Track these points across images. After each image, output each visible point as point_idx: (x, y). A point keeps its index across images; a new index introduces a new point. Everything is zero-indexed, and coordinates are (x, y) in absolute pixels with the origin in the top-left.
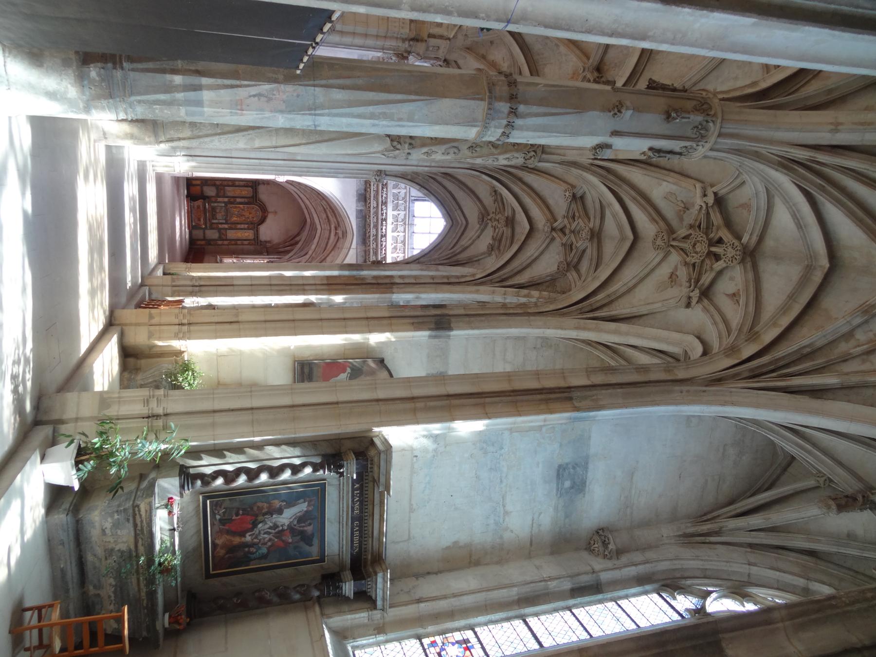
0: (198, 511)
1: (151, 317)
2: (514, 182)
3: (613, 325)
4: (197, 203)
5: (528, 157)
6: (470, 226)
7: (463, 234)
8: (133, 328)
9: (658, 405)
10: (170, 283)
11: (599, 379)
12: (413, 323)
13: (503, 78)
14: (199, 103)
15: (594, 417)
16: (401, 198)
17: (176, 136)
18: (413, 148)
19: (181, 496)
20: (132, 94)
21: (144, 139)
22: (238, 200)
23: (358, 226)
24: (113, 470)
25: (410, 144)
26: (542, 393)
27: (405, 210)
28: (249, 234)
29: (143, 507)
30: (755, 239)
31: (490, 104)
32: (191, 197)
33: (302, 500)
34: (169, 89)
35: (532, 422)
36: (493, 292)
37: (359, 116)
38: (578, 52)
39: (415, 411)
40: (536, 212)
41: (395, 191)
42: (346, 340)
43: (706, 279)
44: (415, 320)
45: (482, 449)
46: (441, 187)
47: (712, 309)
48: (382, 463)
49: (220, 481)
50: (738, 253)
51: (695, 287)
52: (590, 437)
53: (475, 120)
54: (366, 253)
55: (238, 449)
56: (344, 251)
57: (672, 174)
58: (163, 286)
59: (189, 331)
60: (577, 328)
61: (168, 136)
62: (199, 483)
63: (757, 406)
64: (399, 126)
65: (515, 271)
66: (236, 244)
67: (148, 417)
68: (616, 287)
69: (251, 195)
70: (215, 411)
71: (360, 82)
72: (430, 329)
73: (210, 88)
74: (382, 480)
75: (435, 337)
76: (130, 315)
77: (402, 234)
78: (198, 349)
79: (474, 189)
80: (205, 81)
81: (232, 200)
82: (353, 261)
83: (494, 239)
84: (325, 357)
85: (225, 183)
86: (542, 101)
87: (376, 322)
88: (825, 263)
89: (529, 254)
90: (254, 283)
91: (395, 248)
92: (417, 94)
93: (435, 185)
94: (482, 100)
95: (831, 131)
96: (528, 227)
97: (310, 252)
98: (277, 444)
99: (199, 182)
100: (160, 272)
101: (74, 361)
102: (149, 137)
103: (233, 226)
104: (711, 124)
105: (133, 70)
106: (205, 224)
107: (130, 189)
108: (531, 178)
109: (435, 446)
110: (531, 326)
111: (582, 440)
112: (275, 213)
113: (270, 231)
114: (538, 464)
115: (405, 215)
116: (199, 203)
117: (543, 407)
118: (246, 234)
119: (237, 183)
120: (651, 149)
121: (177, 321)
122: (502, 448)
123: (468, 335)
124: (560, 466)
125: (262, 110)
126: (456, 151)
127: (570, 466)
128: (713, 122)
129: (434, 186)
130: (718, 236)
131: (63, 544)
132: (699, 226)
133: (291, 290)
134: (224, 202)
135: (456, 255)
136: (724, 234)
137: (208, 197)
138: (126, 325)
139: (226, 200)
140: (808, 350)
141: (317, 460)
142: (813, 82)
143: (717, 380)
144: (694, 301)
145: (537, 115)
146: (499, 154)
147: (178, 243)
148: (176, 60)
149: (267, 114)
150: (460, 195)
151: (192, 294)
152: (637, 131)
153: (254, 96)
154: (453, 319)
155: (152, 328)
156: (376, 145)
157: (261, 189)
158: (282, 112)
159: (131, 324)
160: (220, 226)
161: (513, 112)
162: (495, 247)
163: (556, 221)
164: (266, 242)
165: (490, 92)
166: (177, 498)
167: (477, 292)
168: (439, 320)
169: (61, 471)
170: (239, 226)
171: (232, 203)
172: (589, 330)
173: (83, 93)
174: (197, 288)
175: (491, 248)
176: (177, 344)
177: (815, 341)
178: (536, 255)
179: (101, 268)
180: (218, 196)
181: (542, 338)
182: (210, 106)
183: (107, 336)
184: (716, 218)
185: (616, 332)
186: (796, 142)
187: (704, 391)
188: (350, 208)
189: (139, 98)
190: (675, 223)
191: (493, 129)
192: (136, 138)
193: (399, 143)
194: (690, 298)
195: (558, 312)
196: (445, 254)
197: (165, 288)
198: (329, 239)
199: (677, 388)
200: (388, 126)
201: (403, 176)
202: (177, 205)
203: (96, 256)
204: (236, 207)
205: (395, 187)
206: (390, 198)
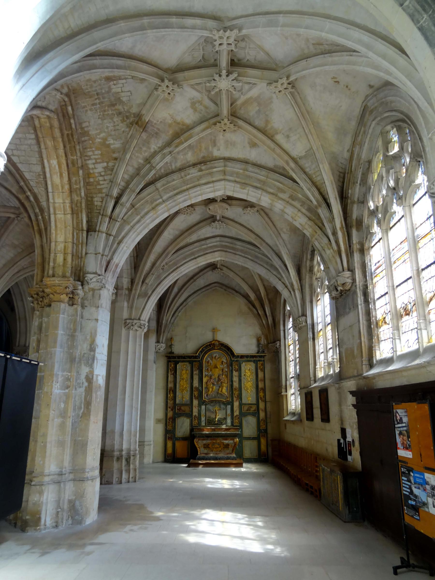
4: (201, 451)
22: (196, 383)
28: (248, 369)
66: (264, 390)
81: (196, 393)
85: (170, 403)
99: (170, 444)
103: (236, 393)
106: (233, 436)
112: (214, 330)
113: (243, 338)
116: (199, 444)
118: (248, 374)
119: (171, 385)
134: (200, 406)
137: (192, 430)
139: (195, 402)
160: (236, 413)
164: (259, 344)
170: (236, 385)
180: (190, 415)
198: (246, 162)
204: (207, 388)
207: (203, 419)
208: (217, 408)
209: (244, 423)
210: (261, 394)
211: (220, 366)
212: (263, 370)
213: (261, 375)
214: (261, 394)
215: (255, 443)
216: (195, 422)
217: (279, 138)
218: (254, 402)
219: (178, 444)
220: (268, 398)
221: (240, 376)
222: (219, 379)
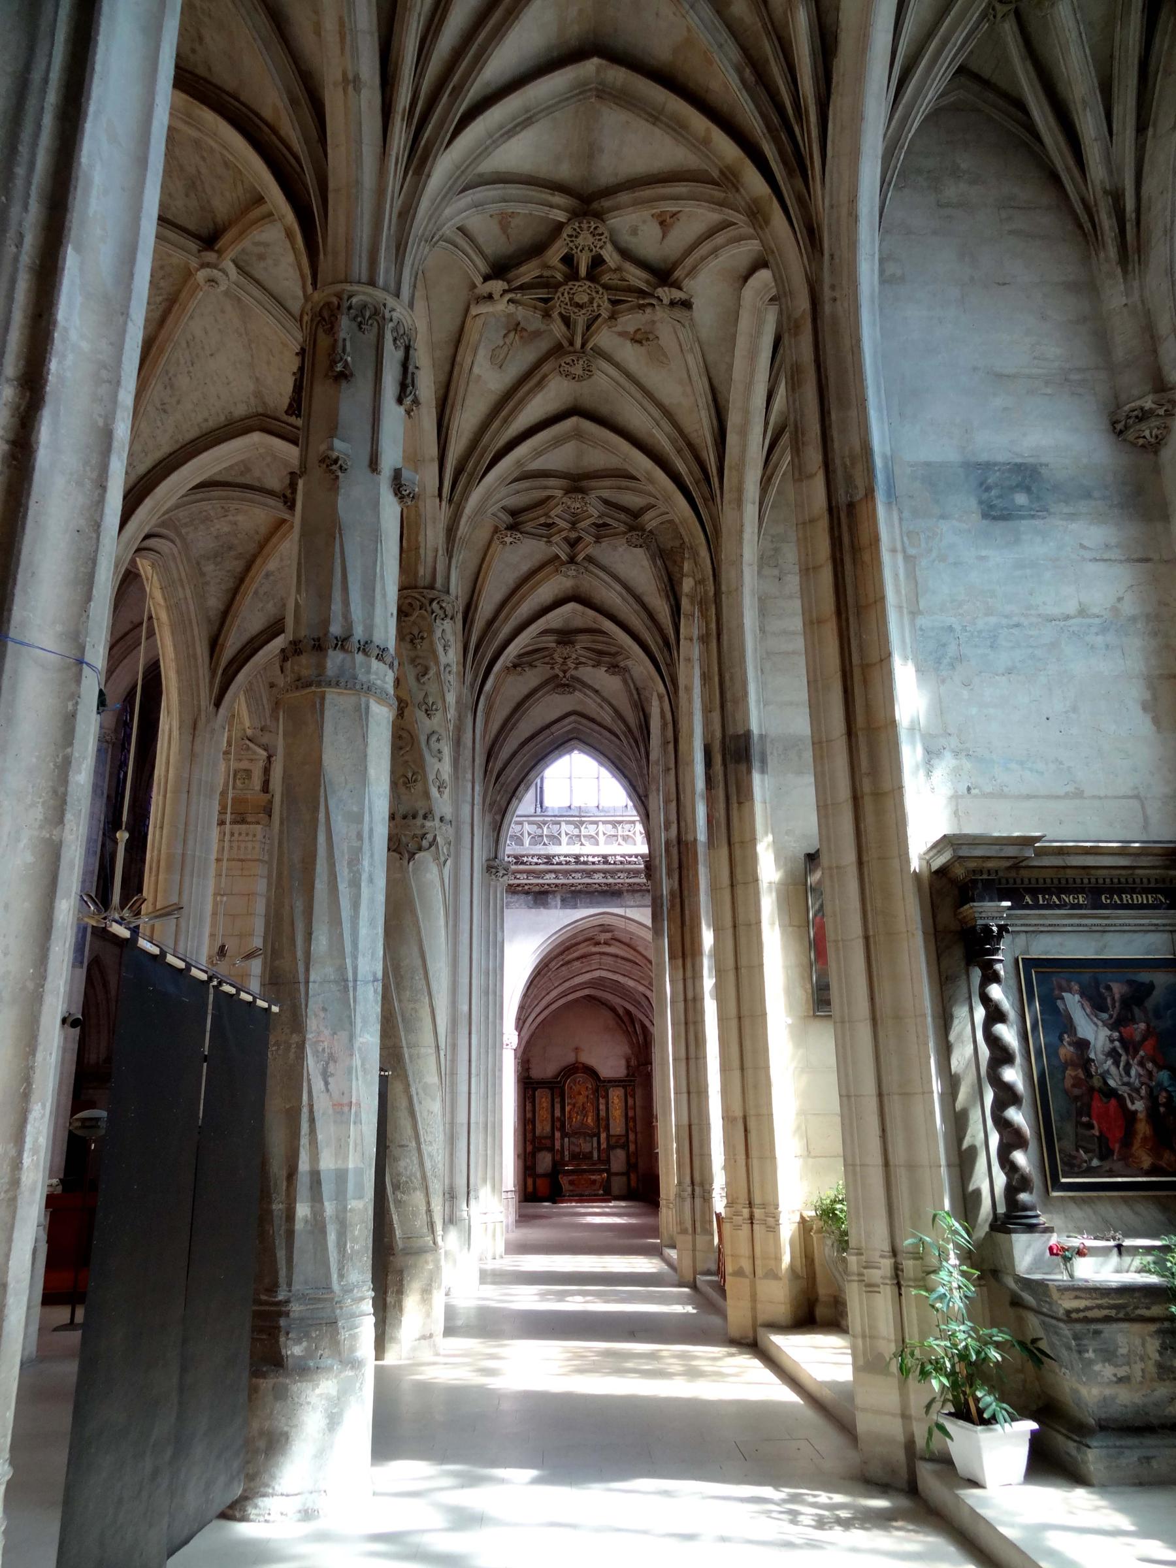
0: (1084, 1200)
1: (739, 1273)
2: (496, 634)
3: (732, 439)
5: (441, 613)
6: (578, 708)
7: (593, 720)
8: (759, 1306)
9: (859, 340)
10: (689, 1238)
11: (813, 457)
12: (740, 803)
13: (288, 664)
14: (341, 1176)
15: (884, 457)
16: (539, 832)
17: (423, 1216)
18: (431, 811)
19: (1049, 1230)
20: (328, 1288)
21: (431, 1271)
22: (558, 1113)
23: (591, 905)
24: (995, 1355)
25: (425, 817)
26: (842, 560)
27: (559, 823)
28: (616, 1096)
29: (1069, 1303)
30: (559, 199)
31: (329, 684)
32: (555, 1195)
33: (1059, 1002)
34: (318, 1226)
35: (897, 575)
36: (689, 660)
37: (356, 905)
38: (274, 540)
39: (878, 795)
40: (545, 592)
41: (527, 841)
42: (773, 924)
43: (636, 277)
44: (734, 799)
45: (952, 667)
46: (513, 762)
47: (689, 262)
48: (979, 852)
49: (1020, 1158)
50: (585, 226)
51: (652, 295)
52: (928, 464)
53: (357, 708)
54: (634, 890)
55: (958, 1122)
56: (632, 928)
57: (458, 359)
58: (694, 1250)
59: (764, 1206)
60: (739, 502)
61: (425, 1230)
62: (1023, 1197)
63: (855, 155)
64: (370, 838)
65: (649, 623)
66: (634, 1119)
67: (899, 1285)
68: (662, 439)
69: (547, 1092)
70: (886, 1164)
71: (299, 905)
72: (749, 772)
73: (315, 1157)
74: (1011, 851)
75: (763, 761)
76: (737, 1313)
77: (601, 827)
78: (799, 1187)
79: (513, 704)
80: (304, 1165)
82: (648, 911)
83: (597, 665)
84: (805, 961)
85: (529, 1136)
86: (324, 598)
87: (738, 870)
88: (591, 66)
89: (619, 601)
90: (684, 1089)
91: (626, 838)
92: (316, 809)
93: (508, 774)
94: (323, 699)
95: (357, 90)
96: (571, 606)
97: (641, 989)
98: (945, 1050)
99: (530, 1181)
100: (673, 1254)
101: (810, 1414)
102: (427, 1262)
103: (603, 1123)
104: (354, 300)
105: (289, 1284)
106: (600, 1171)
107: (528, 1299)
108: (486, 607)
109: (948, 755)
110: (739, 589)
111: (932, 477)
112: (577, 1050)
113: (608, 1058)
114: (982, 558)
115: (568, 823)
116: (564, 1181)
117: (866, 557)
118: (616, 1101)
119: (529, 1115)
120: (400, 401)
121: (746, 1227)
122: (951, 629)
123: (758, 701)
124: (985, 516)
125: (349, 1071)
126: (434, 738)
127: (985, 496)
128: (350, 297)
129: (512, 773)
130: (560, 266)
131: (1148, 1459)
132: (546, 301)
133: (695, 1023)
134: (562, 1138)
135: (630, 730)
136: (554, 255)
138: (754, 1318)
139: (558, 1135)
140: (748, 72)
141: (976, 974)
142: (282, 133)
143: (812, 236)
144: (677, 295)
145: (346, 603)
146: (437, 663)
147: (633, 1221)
148: (270, 1212)
149: (357, 1061)
150: (525, 728)
151: (707, 1198)
152: (368, 427)
153: (327, 1084)
154: (731, 731)
155: (760, 1272)
156: (428, 876)
157: (536, 1073)
158: (351, 1038)
159: (754, 1309)
160: (604, 1146)
161: (342, 643)
162: (612, 661)
163: (557, 557)
164: (628, 1066)
165: (309, 685)
166: (1054, 1239)
167: (688, 689)
168: (734, 755)
169: (1000, 1450)
170: (603, 1113)
171: (562, 1128)
172: (741, 483)
173: (329, 1369)
174: (697, 1189)
175: (614, 668)
176: (788, 1229)
177: (730, 60)
178: (619, 588)
179: (653, 1356)
180: (551, 1149)
181: (760, 568)
182: (346, 1158)
183: (773, 1352)
184: (528, 272)
185: (743, 433)
186: (379, 150)
187: (832, 256)
188: (558, 920)
189: (335, 1277)
190: (544, 345)
191: (373, 677)
192: (430, 1285)
193: (423, 836)
194: (672, 304)
195: (713, 540)
196: (631, 752)
197: (698, 1247)
198: (616, 956)
199: (827, 308)
200: (372, 856)
201: (497, 828)
202: (566, 1219)
203: (630, 1365)
204: (570, 1118)
205: (519, 841)
206: (540, 850)
207: (566, 1153)
208: (581, 1141)
209: (612, 1157)
210: (631, 1124)
211: (584, 1093)
212: (633, 1096)
213: (630, 1101)
214: (631, 1124)
215: (624, 1179)
216: (558, 1157)
217: (639, 948)
218: (624, 1132)
219: (539, 1181)
220: (639, 1129)
221: (607, 1104)
222: (584, 1108)
